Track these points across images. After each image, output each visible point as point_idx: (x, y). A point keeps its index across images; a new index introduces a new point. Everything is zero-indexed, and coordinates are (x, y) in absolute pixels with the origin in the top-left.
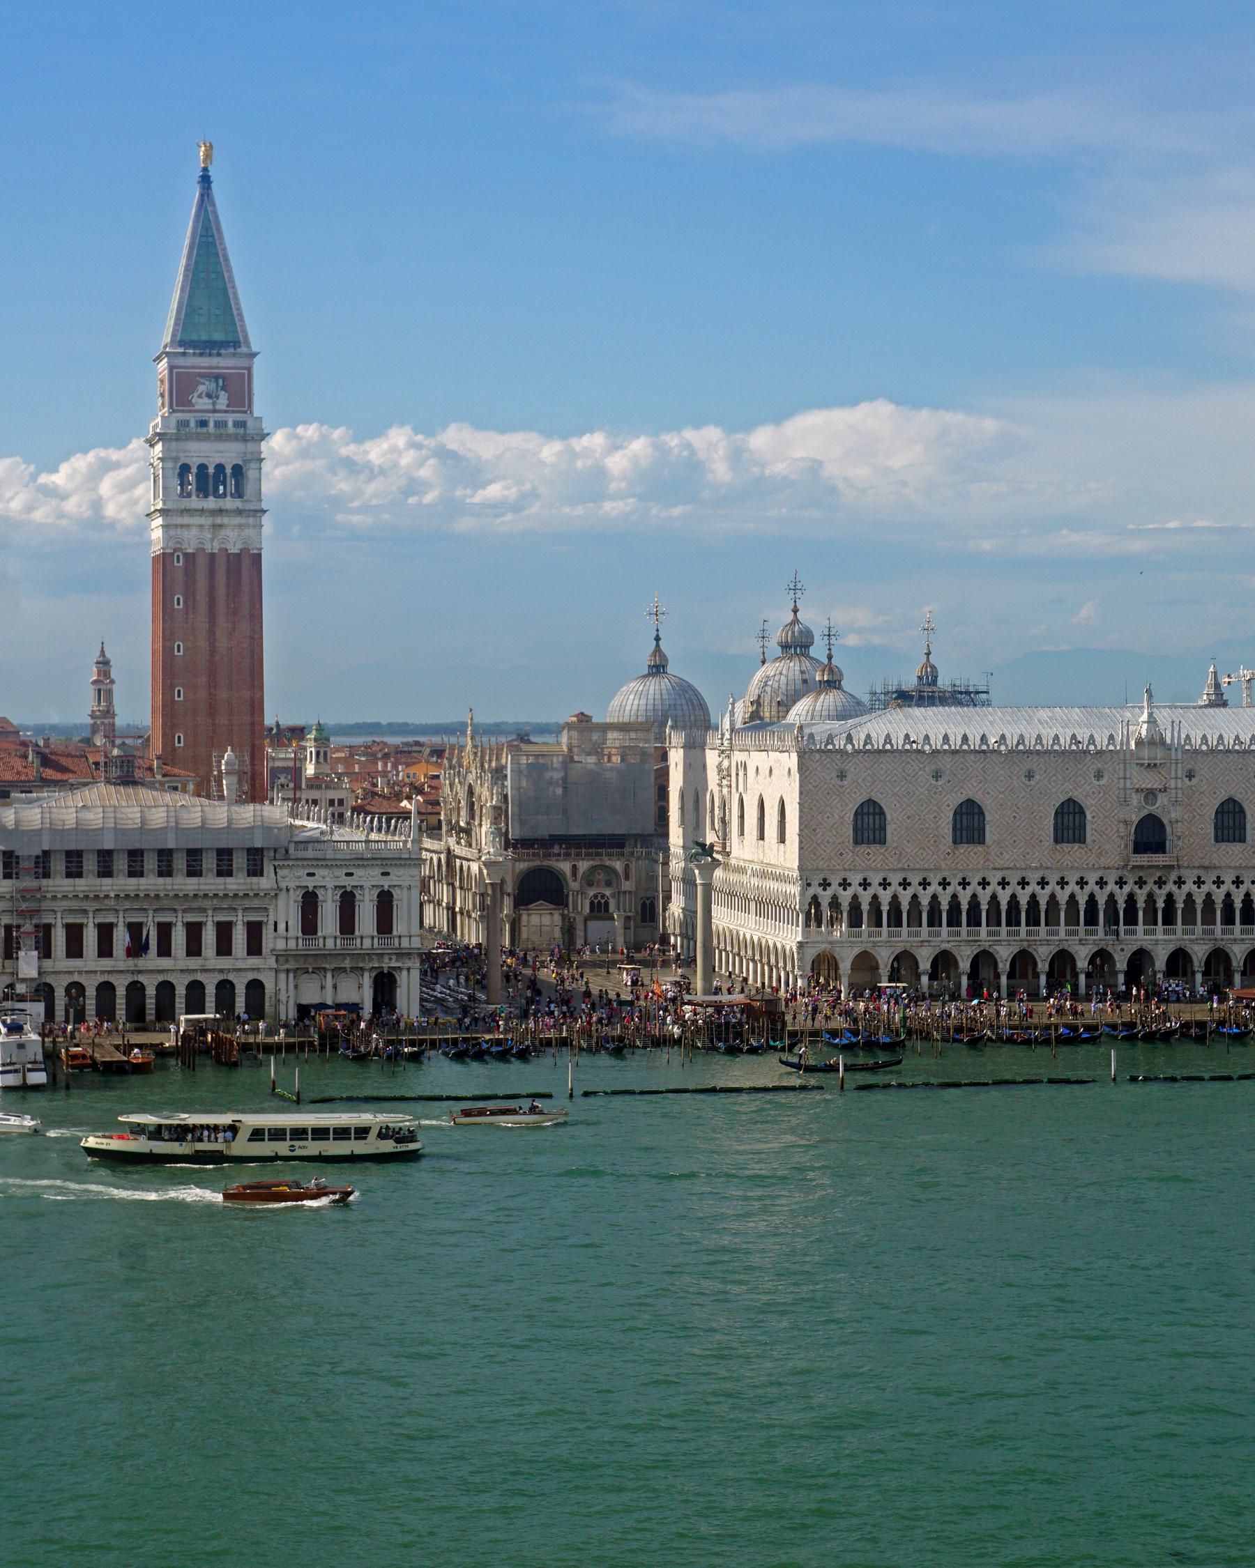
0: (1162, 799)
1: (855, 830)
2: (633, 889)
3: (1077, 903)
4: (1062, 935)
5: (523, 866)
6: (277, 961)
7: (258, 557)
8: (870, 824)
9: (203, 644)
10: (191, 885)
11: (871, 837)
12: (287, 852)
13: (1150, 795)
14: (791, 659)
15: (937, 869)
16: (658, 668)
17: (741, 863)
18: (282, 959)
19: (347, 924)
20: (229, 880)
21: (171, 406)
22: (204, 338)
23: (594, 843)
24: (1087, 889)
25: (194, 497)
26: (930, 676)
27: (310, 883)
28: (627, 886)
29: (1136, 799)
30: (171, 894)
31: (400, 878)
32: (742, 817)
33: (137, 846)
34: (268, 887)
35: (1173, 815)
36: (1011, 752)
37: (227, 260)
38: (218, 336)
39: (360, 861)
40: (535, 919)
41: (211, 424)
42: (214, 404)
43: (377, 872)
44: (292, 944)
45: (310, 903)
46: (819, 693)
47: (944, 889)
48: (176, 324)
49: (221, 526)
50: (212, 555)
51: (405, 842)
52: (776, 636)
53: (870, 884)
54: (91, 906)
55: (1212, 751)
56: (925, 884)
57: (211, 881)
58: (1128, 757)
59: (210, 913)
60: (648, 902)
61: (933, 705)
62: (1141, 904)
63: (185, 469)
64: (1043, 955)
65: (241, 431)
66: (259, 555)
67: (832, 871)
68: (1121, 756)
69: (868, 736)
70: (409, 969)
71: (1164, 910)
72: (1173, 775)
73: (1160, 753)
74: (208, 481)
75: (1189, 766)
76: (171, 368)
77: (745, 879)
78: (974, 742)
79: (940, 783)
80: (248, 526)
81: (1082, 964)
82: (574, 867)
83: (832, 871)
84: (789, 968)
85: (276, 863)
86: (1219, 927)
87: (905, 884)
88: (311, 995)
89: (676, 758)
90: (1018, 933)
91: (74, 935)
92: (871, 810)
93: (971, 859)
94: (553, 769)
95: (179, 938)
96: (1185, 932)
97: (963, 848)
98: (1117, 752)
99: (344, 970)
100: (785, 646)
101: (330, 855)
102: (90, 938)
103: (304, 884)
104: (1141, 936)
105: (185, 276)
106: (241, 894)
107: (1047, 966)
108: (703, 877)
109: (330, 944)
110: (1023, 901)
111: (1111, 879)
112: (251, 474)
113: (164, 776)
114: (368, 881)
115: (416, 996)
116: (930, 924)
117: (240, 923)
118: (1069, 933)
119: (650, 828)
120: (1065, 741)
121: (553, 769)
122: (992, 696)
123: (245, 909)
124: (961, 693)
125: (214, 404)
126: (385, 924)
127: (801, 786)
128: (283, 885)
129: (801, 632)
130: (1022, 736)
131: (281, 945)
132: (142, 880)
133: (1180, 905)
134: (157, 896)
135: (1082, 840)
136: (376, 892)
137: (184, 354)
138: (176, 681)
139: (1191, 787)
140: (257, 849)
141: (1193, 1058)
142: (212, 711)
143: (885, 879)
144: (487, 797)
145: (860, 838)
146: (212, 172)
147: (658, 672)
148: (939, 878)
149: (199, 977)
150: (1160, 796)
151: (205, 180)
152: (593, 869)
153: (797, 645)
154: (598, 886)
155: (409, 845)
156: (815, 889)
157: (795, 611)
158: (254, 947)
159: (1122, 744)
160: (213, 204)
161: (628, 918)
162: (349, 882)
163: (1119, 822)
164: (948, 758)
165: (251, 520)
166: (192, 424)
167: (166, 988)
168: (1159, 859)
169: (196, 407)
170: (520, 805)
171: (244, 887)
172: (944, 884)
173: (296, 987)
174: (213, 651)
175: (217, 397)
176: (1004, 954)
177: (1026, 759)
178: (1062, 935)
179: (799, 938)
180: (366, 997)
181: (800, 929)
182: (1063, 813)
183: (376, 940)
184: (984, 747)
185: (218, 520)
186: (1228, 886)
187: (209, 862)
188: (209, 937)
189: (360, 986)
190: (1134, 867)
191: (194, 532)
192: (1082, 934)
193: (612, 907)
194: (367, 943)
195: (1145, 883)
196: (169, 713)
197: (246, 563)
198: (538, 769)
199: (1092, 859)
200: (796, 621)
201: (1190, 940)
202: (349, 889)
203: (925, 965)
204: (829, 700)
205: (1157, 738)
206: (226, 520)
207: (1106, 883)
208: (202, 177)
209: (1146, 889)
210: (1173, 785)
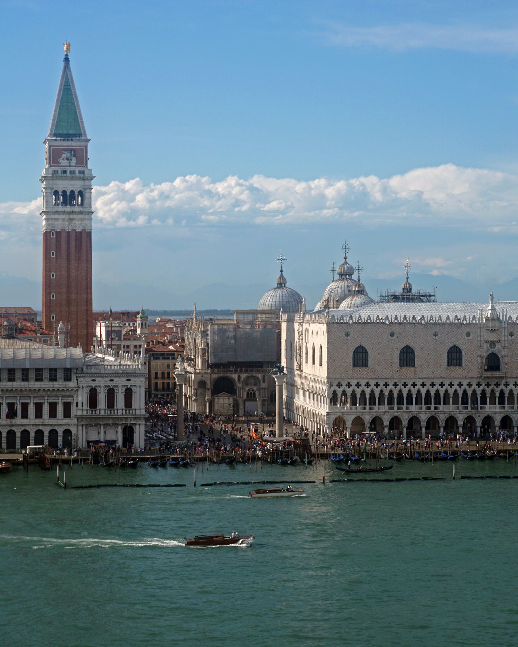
0: (498, 346)
1: (354, 360)
2: (267, 387)
3: (458, 394)
4: (451, 409)
5: (215, 376)
6: (77, 421)
7: (89, 234)
8: (361, 357)
9: (64, 273)
11: (361, 363)
12: (82, 369)
13: (492, 344)
14: (343, 280)
15: (392, 378)
16: (282, 284)
17: (307, 375)
18: (80, 420)
19: (111, 403)
20: (55, 383)
21: (50, 164)
22: (65, 132)
23: (248, 364)
24: (463, 388)
25: (60, 206)
26: (408, 289)
27: (93, 384)
28: (264, 385)
29: (486, 346)
30: (28, 389)
32: (307, 354)
33: (11, 367)
34: (74, 386)
35: (503, 353)
36: (427, 324)
37: (76, 97)
38: (71, 132)
39: (117, 374)
40: (221, 401)
41: (68, 172)
42: (70, 163)
43: (125, 379)
46: (354, 296)
47: (396, 387)
48: (52, 126)
49: (73, 219)
50: (69, 232)
51: (138, 365)
52: (338, 269)
53: (379, 385)
56: (386, 385)
57: (47, 383)
58: (482, 326)
59: (46, 398)
60: (274, 393)
61: (409, 302)
62: (488, 395)
64: (442, 418)
65: (82, 175)
66: (91, 232)
67: (343, 379)
68: (479, 326)
69: (360, 316)
70: (139, 425)
71: (499, 398)
72: (503, 335)
73: (497, 324)
74: (68, 198)
75: (511, 330)
76: (50, 146)
77: (308, 382)
78: (410, 319)
79: (393, 338)
80: (85, 219)
81: (460, 423)
82: (239, 377)
83: (343, 379)
84: (323, 424)
85: (77, 375)
87: (377, 385)
88: (93, 436)
89: (284, 326)
90: (430, 408)
92: (361, 351)
94: (229, 331)
95: (32, 410)
96: (509, 408)
97: (404, 369)
98: (477, 324)
99: (109, 425)
100: (341, 275)
101: (102, 371)
103: (90, 385)
104: (488, 410)
105: (57, 104)
106: (61, 389)
107: (444, 424)
108: (278, 382)
109: (102, 412)
110: (433, 393)
111: (474, 383)
112: (87, 195)
113: (41, 334)
114: (120, 383)
115: (143, 437)
117: (60, 403)
119: (275, 359)
120: (452, 319)
121: (229, 331)
122: (437, 298)
123: (63, 397)
124: (422, 296)
125: (70, 163)
126: (128, 403)
127: (328, 339)
128: (80, 385)
129: (348, 268)
130: (432, 316)
131: (79, 413)
132: (14, 383)
133: (507, 395)
134: (21, 390)
135: (460, 365)
136: (124, 389)
137: (56, 140)
138: (52, 290)
139: (512, 340)
140: (68, 369)
141: (501, 467)
142: (68, 304)
143: (368, 383)
144: (200, 344)
145: (356, 364)
146: (69, 57)
147: (282, 287)
148: (393, 383)
149: (41, 428)
150: (497, 344)
151: (67, 60)
152: (248, 378)
153: (346, 274)
154: (251, 385)
155: (140, 367)
157: (346, 258)
158: (67, 414)
159: (479, 320)
160: (70, 71)
161: (264, 401)
163: (478, 356)
164: (397, 327)
165: (87, 217)
166: (60, 172)
167: (25, 434)
168: (497, 374)
169: (62, 164)
170: (214, 348)
171: (62, 386)
172: (396, 385)
173: (87, 433)
174: (69, 276)
175: (71, 160)
176: (424, 418)
177: (434, 327)
178: (451, 409)
179: (328, 411)
181: (328, 406)
182: (451, 352)
183: (124, 411)
184: (414, 322)
185: (72, 216)
187: (46, 374)
188: (46, 409)
189: (117, 433)
191: (60, 222)
192: (460, 409)
193: (257, 395)
194: (120, 412)
195: (490, 385)
196: (48, 304)
197: (84, 236)
198: (222, 331)
199: (465, 374)
200: (346, 263)
201: (512, 412)
202: (111, 387)
203: (386, 423)
204: (358, 299)
205: (496, 318)
206: (75, 216)
207: (472, 385)
208: (65, 58)
209: (491, 388)
210: (503, 339)
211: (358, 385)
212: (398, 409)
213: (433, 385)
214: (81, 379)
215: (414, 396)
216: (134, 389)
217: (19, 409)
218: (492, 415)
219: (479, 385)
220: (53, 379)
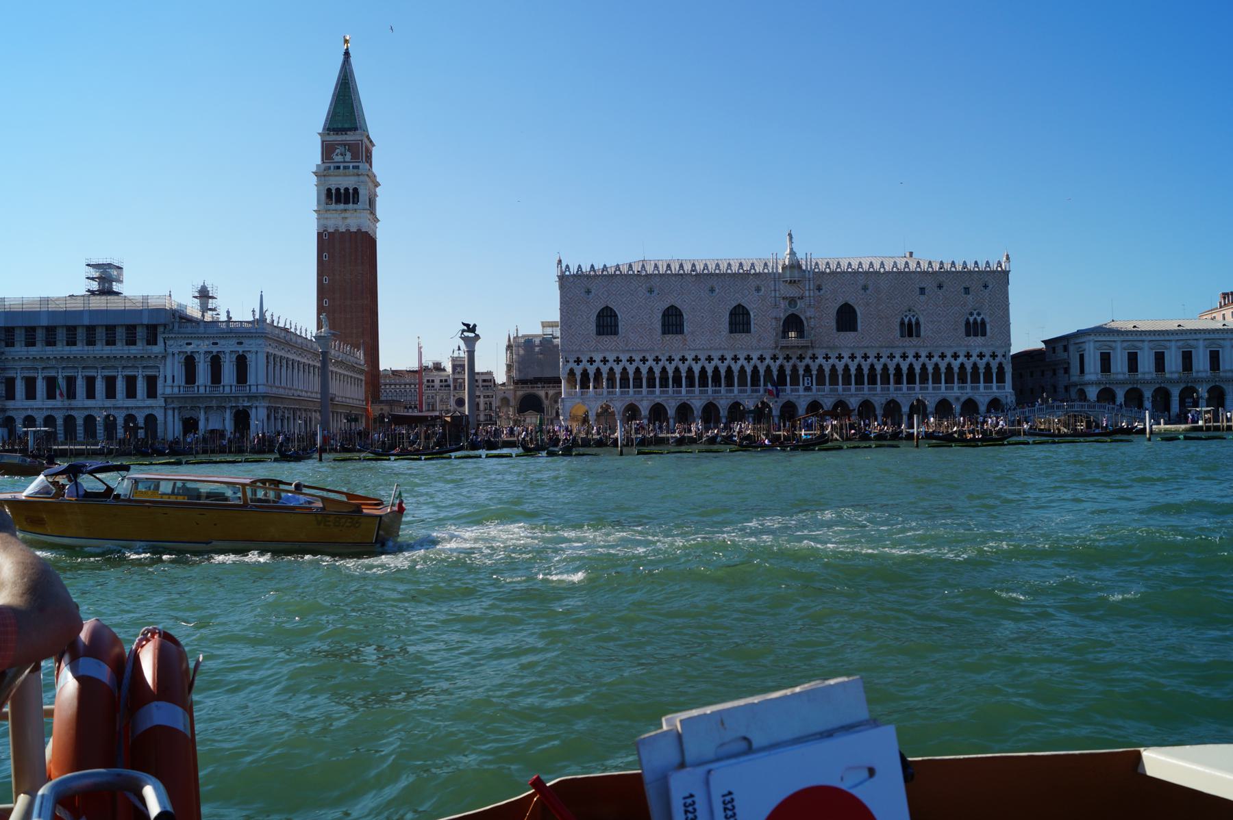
4: (736, 392)
5: (520, 393)
8: (607, 322)
10: (108, 350)
13: (792, 301)
19: (216, 377)
20: (133, 347)
24: (752, 362)
29: (783, 304)
31: (250, 346)
38: (346, 126)
43: (234, 341)
44: (176, 390)
45: (190, 363)
54: (39, 365)
55: (833, 273)
56: (644, 360)
62: (788, 372)
63: (329, 190)
68: (774, 277)
73: (796, 273)
86: (840, 387)
91: (30, 384)
93: (674, 346)
95: (100, 386)
96: (818, 390)
97: (668, 337)
102: (41, 387)
116: (648, 386)
118: (740, 391)
126: (242, 376)
128: (170, 350)
131: (168, 391)
136: (234, 356)
148: (653, 356)
151: (347, 54)
156: (572, 365)
158: (152, 393)
160: (350, 65)
162: (215, 349)
172: (657, 360)
178: (736, 392)
180: (229, 426)
186: (846, 360)
188: (120, 386)
190: (782, 347)
209: (791, 362)
211: (605, 361)
212: (662, 392)
213: (709, 359)
214: (171, 342)
215: (684, 375)
216: (248, 356)
217: (62, 383)
218: (793, 399)
219: (774, 358)
220: (131, 341)
